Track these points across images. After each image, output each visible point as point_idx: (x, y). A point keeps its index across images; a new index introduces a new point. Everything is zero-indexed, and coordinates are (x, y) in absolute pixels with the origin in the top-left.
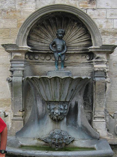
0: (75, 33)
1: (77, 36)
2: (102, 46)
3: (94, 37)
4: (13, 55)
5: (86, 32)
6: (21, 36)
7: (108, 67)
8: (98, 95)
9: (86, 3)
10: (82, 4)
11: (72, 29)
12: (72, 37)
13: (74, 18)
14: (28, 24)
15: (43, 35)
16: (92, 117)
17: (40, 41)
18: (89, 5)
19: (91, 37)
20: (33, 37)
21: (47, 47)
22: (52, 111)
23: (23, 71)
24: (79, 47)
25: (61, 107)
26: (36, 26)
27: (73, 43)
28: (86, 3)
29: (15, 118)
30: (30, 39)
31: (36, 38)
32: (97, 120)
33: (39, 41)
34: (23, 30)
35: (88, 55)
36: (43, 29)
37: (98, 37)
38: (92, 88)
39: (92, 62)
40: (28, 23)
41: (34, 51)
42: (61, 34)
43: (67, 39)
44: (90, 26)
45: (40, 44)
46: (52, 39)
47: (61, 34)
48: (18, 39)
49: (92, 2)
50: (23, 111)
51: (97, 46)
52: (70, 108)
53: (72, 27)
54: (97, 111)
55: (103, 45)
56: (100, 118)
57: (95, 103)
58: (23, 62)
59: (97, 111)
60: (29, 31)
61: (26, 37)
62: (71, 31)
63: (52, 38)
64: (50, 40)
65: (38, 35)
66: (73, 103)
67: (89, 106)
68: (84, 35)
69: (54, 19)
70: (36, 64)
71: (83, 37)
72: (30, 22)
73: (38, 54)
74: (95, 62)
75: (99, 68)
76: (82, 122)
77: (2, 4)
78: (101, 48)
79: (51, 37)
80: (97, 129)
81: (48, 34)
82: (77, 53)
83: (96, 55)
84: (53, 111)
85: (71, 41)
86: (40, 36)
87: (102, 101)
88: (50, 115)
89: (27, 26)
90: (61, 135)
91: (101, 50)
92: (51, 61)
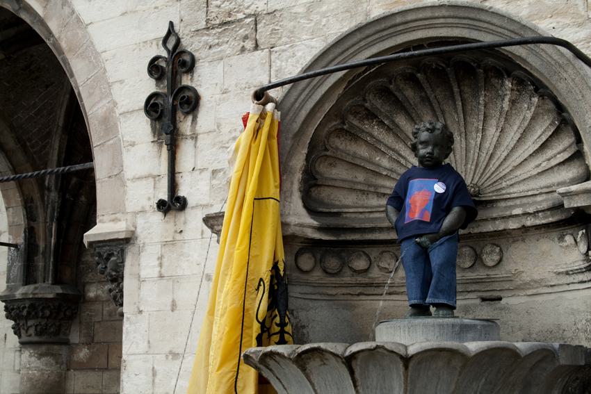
15: (385, 162)
17: (372, 189)
26: (340, 127)
27: (517, 180)
30: (320, 183)
31: (349, 177)
41: (339, 235)
47: (425, 143)
53: (502, 108)
60: (305, 151)
65: (358, 162)
69: (411, 79)
73: (366, 250)
77: (282, 61)
85: (508, 170)
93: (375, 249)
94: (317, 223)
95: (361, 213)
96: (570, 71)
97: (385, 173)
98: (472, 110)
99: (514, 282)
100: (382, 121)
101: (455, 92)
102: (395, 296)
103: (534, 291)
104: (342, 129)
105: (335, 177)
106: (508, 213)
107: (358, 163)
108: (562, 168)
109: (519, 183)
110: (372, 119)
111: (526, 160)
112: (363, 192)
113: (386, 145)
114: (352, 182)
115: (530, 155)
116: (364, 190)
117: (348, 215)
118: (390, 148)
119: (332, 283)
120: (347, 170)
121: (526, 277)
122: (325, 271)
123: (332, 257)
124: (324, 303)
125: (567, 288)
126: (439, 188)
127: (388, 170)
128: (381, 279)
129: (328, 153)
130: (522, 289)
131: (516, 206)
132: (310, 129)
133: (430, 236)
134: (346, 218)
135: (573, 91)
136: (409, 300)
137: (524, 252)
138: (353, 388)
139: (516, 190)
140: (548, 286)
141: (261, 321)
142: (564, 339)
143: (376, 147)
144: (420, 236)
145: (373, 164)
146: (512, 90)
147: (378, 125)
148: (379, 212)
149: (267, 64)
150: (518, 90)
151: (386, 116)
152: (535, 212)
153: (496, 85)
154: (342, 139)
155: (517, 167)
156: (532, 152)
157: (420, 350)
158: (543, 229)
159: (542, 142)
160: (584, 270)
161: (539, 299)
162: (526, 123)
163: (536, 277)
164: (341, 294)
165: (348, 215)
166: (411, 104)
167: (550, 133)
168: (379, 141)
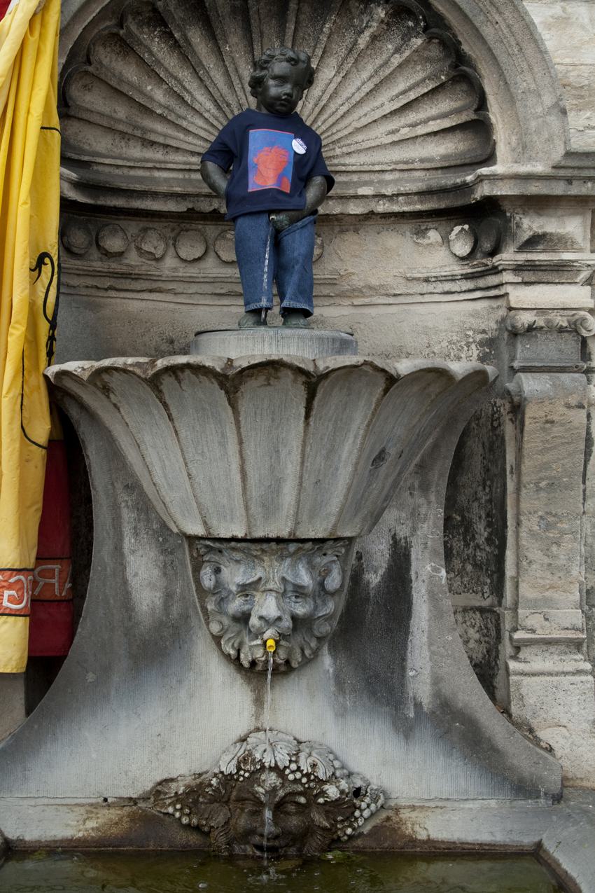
1: (386, 101)
2: (563, 163)
3: (510, 99)
8: (539, 489)
11: (351, 51)
12: (354, 106)
15: (159, 95)
16: (499, 638)
17: (138, 133)
19: (482, 105)
20: (92, 100)
21: (180, 175)
22: (236, 605)
24: (397, 175)
25: (297, 575)
26: (115, 30)
27: (359, 147)
30: (72, 113)
31: (106, 110)
32: (537, 661)
36: (155, 49)
38: (495, 447)
41: (97, 197)
42: (282, 79)
45: (136, 151)
46: (217, 119)
51: (530, 159)
52: (356, 578)
53: (355, 43)
54: (536, 600)
55: (569, 154)
56: (552, 649)
59: (534, 604)
62: (347, 66)
63: (214, 110)
64: (206, 126)
65: (125, 89)
66: (379, 552)
67: (469, 567)
68: (433, 92)
70: (111, 288)
74: (518, 269)
75: (541, 311)
76: (436, 680)
78: (562, 173)
79: (209, 105)
80: (534, 723)
81: (191, 84)
82: (386, 216)
83: (518, 226)
84: (246, 608)
85: (346, 132)
87: (563, 533)
88: (217, 639)
90: (298, 775)
91: (559, 189)
92: (210, 268)
93: (133, 223)
94: (74, 175)
95: (118, 166)
96: (507, 14)
97: (159, 111)
98: (304, 38)
99: (338, 287)
100: (171, 31)
101: (291, 9)
102: (158, 294)
103: (366, 301)
104: (117, 35)
105: (88, 106)
106: (351, 192)
107: (125, 91)
108: (430, 139)
109: (359, 151)
110: (155, 27)
111: (375, 121)
112: (123, 135)
113: (166, 70)
115: (385, 116)
116: (126, 133)
117: (100, 168)
118: (171, 75)
119: (77, 269)
120: (105, 98)
121: (357, 282)
123: (79, 229)
125: (420, 299)
126: (299, 147)
127: (165, 107)
128: (143, 268)
129: (91, 69)
130: (347, 297)
131: (366, 184)
132: (76, 27)
133: (293, 213)
134: (97, 172)
135: (505, 41)
136: (246, 304)
137: (356, 247)
138: (303, 419)
139: (354, 161)
140: (388, 295)
141: (50, 319)
143: (153, 70)
144: (278, 212)
145: (142, 93)
146: (382, 21)
147: (160, 37)
148: (143, 168)
150: (388, 24)
151: (179, 26)
152: (393, 195)
154: (108, 49)
155: (358, 130)
156: (388, 111)
157: (414, 370)
158: (392, 219)
159: (408, 100)
160: (460, 277)
161: (372, 311)
162: (388, 71)
163: (374, 282)
164: (83, 287)
165: (100, 168)
166: (218, 15)
167: (426, 90)
168: (158, 62)
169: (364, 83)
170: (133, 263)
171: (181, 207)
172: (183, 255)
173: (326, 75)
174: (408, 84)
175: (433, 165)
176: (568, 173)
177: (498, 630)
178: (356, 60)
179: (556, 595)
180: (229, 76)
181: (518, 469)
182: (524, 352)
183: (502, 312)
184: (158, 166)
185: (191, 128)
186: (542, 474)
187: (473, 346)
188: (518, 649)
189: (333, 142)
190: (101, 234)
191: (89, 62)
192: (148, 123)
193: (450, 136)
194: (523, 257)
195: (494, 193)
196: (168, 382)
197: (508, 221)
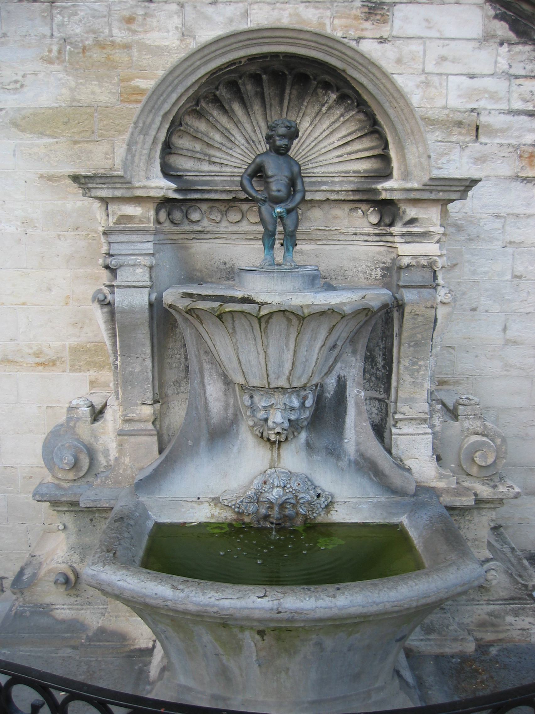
0: (328, 128)
1: (336, 139)
2: (428, 183)
3: (401, 148)
4: (114, 213)
5: (371, 129)
6: (139, 146)
7: (444, 252)
8: (410, 346)
9: (356, 18)
10: (343, 21)
12: (319, 142)
13: (328, 78)
14: (165, 101)
15: (217, 137)
16: (387, 414)
18: (367, 25)
20: (182, 142)
21: (229, 179)
22: (261, 414)
23: (151, 268)
24: (341, 179)
25: (291, 402)
27: (321, 164)
28: (356, 18)
29: (127, 427)
30: (173, 152)
31: (190, 147)
32: (406, 428)
33: (201, 156)
34: (147, 123)
35: (374, 207)
37: (417, 148)
39: (391, 234)
40: (165, 96)
41: (187, 195)
42: (282, 136)
43: (298, 150)
44: (386, 108)
45: (206, 167)
46: (247, 149)
47: (282, 136)
48: (129, 157)
49: (376, 14)
50: (156, 402)
51: (411, 180)
54: (406, 399)
55: (431, 179)
56: (413, 422)
57: (398, 373)
58: (151, 238)
59: (406, 400)
61: (159, 147)
62: (315, 123)
63: (246, 144)
65: (200, 136)
66: (331, 383)
67: (373, 379)
68: (361, 137)
69: (256, 79)
70: (194, 239)
71: (357, 146)
72: (173, 91)
73: (198, 205)
74: (403, 235)
75: (414, 257)
76: (358, 444)
78: (427, 188)
79: (243, 141)
80: (403, 457)
81: (235, 131)
83: (404, 212)
84: (265, 416)
85: (314, 156)
86: (206, 139)
89: (159, 109)
90: (291, 490)
91: (426, 196)
92: (245, 226)
94: (175, 186)
105: (181, 146)
112: (199, 159)
114: (193, 151)
117: (187, 177)
120: (189, 141)
122: (172, 222)
124: (169, 246)
142: (345, 276)
149: (49, 18)
150: (338, 101)
151: (227, 102)
153: (319, 94)
154: (191, 116)
165: (187, 177)
169: (324, 131)
170: (205, 225)
171: (230, 197)
172: (230, 220)
173: (304, 125)
174: (347, 132)
175: (360, 175)
176: (432, 188)
177: (387, 411)
178: (320, 119)
179: (418, 396)
180: (254, 127)
181: (400, 334)
182: (405, 278)
183: (394, 255)
184: (217, 174)
185: (234, 154)
186: (412, 339)
187: (378, 269)
188: (397, 422)
189: (308, 161)
190: (189, 212)
191: (181, 125)
192: (212, 152)
193: (369, 160)
194: (405, 229)
195: (392, 198)
196: (228, 318)
197: (399, 209)
